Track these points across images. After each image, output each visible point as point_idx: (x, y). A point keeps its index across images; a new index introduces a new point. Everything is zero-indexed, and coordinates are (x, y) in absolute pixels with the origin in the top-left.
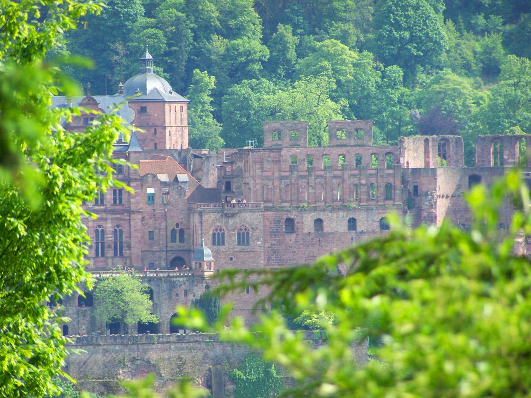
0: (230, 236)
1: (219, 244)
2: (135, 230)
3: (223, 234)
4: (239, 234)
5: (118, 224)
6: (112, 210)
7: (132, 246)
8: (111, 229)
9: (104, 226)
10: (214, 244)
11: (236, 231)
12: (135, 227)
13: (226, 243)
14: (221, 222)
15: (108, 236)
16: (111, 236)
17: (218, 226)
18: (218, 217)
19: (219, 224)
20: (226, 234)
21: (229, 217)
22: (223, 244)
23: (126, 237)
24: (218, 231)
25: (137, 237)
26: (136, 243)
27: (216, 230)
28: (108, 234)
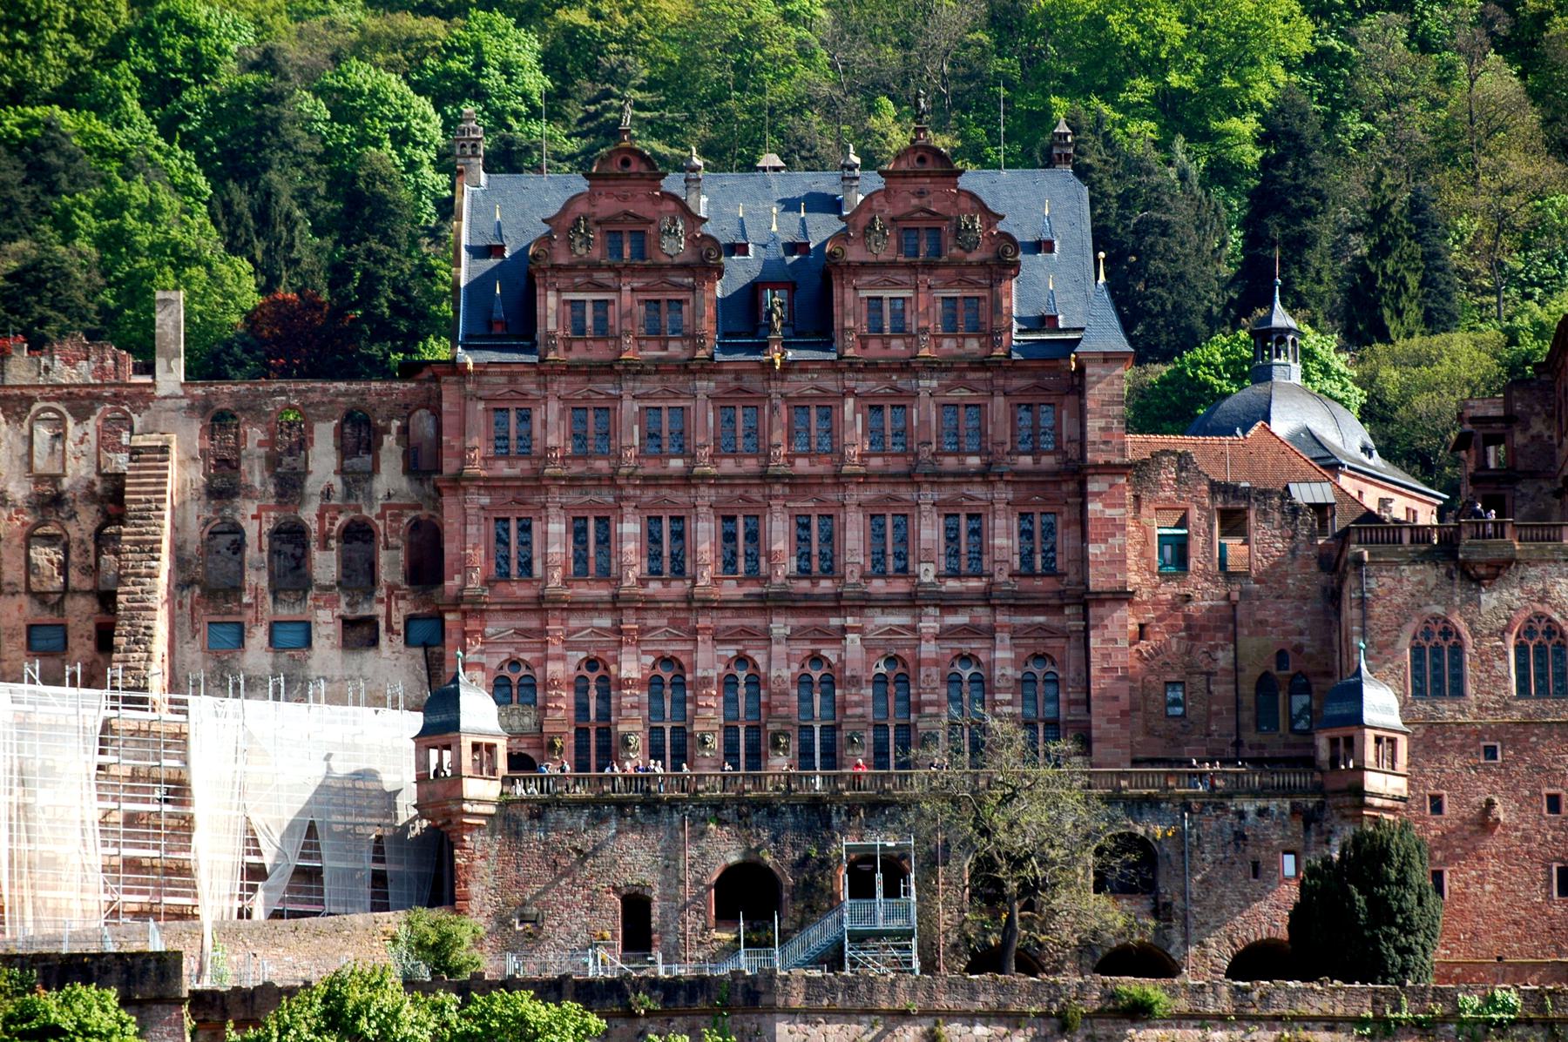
0: (1485, 662)
1: (1439, 692)
2: (1104, 670)
3: (1458, 650)
4: (1521, 650)
5: (1041, 650)
6: (1015, 594)
7: (1095, 733)
8: (1009, 671)
9: (982, 657)
10: (1419, 691)
11: (1511, 640)
12: (1106, 656)
13: (1470, 688)
14: (1448, 603)
15: (998, 697)
16: (1009, 697)
17: (1436, 618)
18: (1432, 582)
19: (1439, 610)
20: (1469, 649)
21: (1478, 581)
22: (1458, 691)
23: (1071, 703)
24: (1437, 638)
25: (1116, 698)
26: (1110, 721)
27: (1427, 634)
28: (1000, 690)
